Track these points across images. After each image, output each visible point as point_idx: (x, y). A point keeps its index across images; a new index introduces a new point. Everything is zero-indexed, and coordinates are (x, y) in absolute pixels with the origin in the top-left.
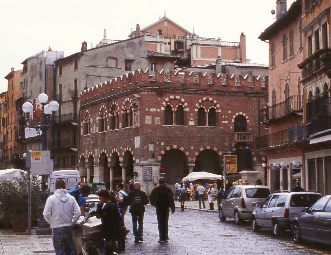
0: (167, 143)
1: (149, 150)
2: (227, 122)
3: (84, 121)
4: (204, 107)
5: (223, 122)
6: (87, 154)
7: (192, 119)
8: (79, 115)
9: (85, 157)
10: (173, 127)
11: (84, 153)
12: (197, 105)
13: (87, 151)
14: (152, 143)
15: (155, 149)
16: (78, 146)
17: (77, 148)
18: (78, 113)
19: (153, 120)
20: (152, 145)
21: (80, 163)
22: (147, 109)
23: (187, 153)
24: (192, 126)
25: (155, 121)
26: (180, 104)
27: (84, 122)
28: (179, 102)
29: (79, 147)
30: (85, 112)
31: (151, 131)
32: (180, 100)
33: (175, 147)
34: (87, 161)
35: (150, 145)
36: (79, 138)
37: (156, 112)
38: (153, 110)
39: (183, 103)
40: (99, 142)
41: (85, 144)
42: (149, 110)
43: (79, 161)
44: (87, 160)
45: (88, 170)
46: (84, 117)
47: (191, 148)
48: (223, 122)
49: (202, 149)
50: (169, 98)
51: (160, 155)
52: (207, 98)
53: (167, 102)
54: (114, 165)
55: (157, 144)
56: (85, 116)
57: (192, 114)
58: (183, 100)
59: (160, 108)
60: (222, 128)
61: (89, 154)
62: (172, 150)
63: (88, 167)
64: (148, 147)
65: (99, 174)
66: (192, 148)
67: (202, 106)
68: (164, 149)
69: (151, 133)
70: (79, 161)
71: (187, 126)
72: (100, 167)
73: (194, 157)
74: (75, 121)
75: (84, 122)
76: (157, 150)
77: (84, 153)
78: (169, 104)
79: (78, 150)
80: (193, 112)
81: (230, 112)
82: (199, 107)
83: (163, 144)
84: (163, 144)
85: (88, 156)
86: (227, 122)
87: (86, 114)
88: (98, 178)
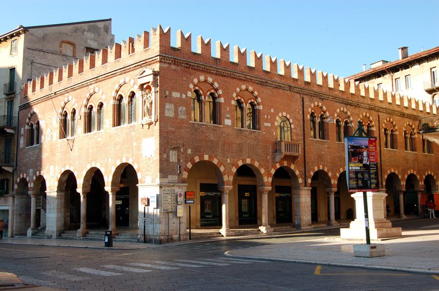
0: (197, 151)
1: (171, 161)
2: (269, 125)
3: (26, 126)
4: (243, 100)
5: (266, 124)
6: (31, 174)
7: (228, 116)
8: (17, 118)
9: (28, 179)
10: (203, 125)
11: (25, 175)
12: (234, 95)
13: (31, 170)
14: (174, 149)
15: (179, 160)
16: (15, 163)
17: (13, 167)
18: (15, 114)
19: (176, 112)
20: (174, 152)
21: (17, 190)
22: (167, 93)
23: (222, 169)
24: (228, 126)
25: (179, 113)
26: (213, 91)
27: (27, 127)
28: (212, 87)
29: (17, 165)
30: (30, 112)
31: (173, 130)
32: (212, 84)
33: (206, 158)
34: (31, 185)
35: (171, 152)
36: (15, 153)
37: (181, 99)
38: (176, 95)
39: (216, 90)
40: (58, 154)
41: (27, 160)
42: (170, 94)
43: (16, 187)
44: (32, 184)
45: (33, 200)
46: (27, 121)
47: (227, 161)
48: (266, 124)
49: (240, 163)
50: (198, 78)
51: (186, 170)
52: (246, 86)
53: (195, 86)
54: (88, 190)
55: (182, 151)
56: (30, 119)
57: (228, 109)
58: (216, 85)
59: (186, 94)
60: (264, 133)
61: (36, 174)
62: (202, 163)
63: (33, 195)
64: (168, 156)
65: (58, 204)
66: (229, 161)
67: (239, 98)
68: (190, 161)
69: (174, 132)
70: (16, 187)
71: (222, 126)
72: (59, 194)
73: (231, 175)
74: (9, 125)
75: (27, 127)
76: (182, 161)
77: (25, 175)
78: (197, 88)
79: (14, 170)
80: (230, 105)
81: (272, 110)
82: (236, 99)
83: (189, 151)
84: (189, 151)
85: (34, 178)
86: (269, 125)
87: (31, 115)
88: (55, 211)
